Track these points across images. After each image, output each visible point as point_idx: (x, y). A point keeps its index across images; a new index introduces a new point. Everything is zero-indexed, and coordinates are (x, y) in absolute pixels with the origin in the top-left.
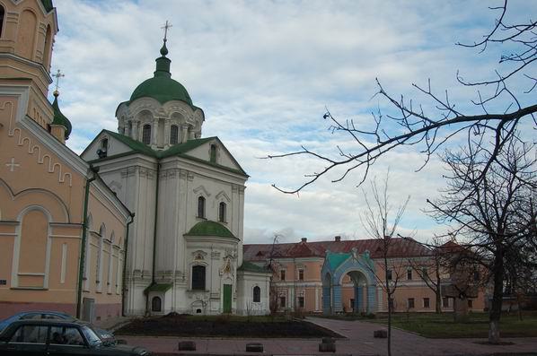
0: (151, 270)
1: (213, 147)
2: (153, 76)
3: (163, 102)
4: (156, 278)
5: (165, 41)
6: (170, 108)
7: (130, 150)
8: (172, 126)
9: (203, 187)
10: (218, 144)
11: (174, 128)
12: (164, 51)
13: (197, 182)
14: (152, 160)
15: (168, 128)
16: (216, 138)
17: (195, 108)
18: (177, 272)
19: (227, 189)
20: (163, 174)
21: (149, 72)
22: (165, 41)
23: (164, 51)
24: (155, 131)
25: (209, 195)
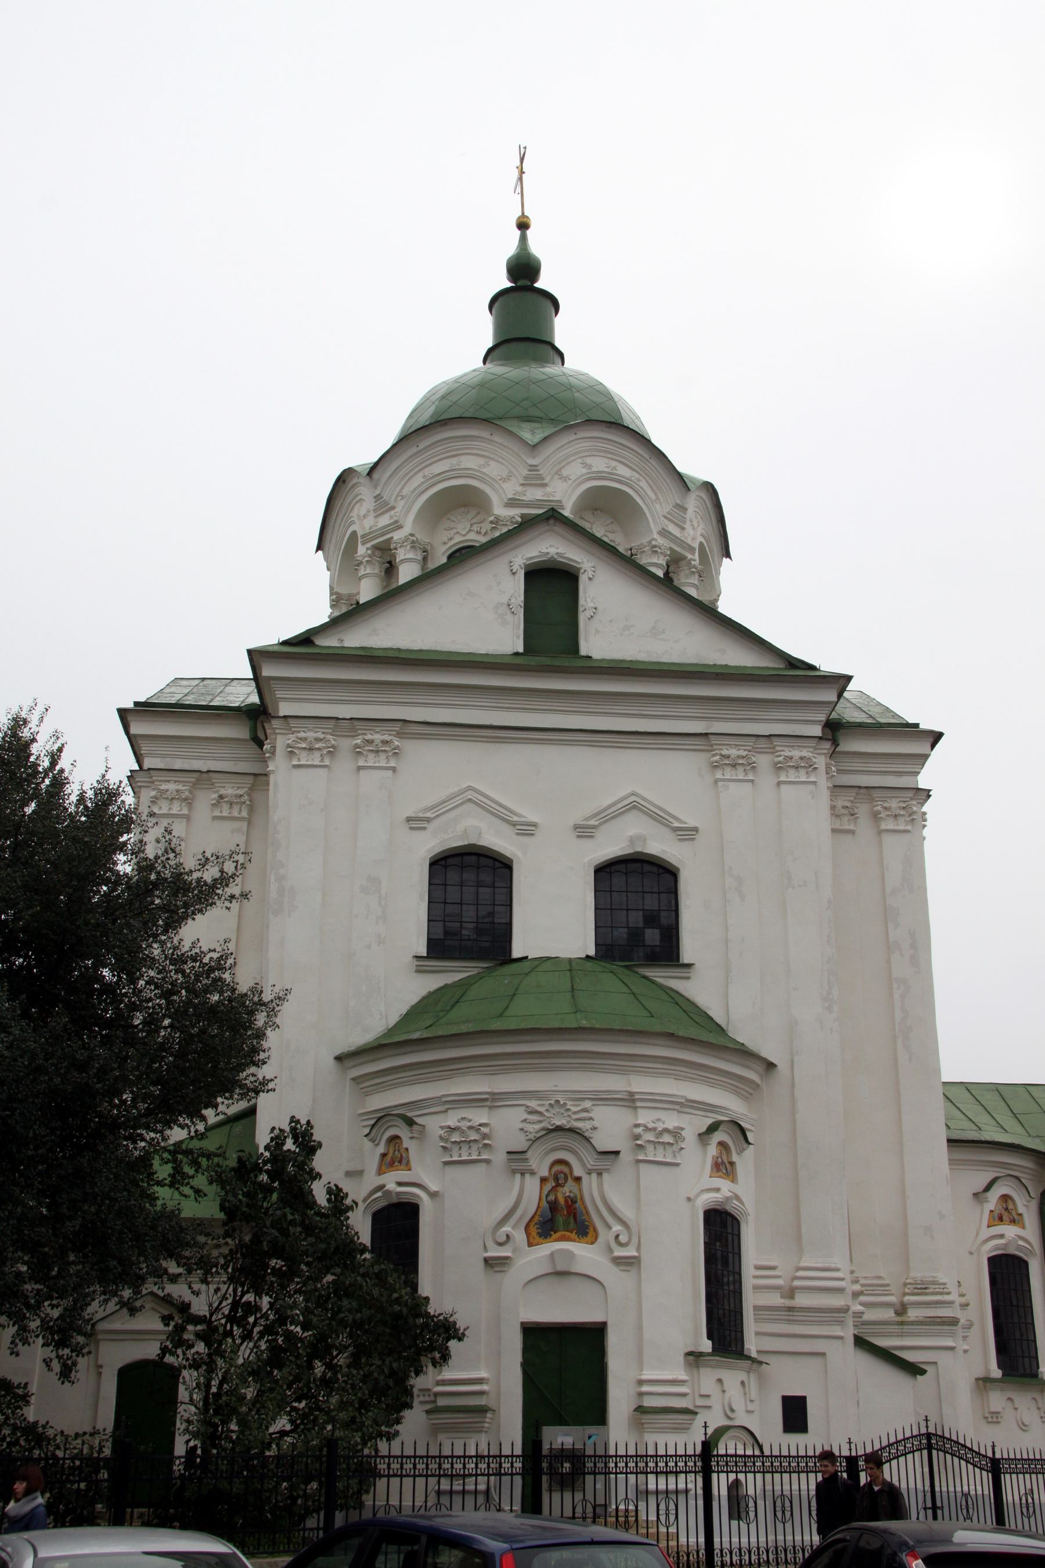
5: (523, 225)
12: (523, 269)
22: (523, 225)
23: (523, 269)
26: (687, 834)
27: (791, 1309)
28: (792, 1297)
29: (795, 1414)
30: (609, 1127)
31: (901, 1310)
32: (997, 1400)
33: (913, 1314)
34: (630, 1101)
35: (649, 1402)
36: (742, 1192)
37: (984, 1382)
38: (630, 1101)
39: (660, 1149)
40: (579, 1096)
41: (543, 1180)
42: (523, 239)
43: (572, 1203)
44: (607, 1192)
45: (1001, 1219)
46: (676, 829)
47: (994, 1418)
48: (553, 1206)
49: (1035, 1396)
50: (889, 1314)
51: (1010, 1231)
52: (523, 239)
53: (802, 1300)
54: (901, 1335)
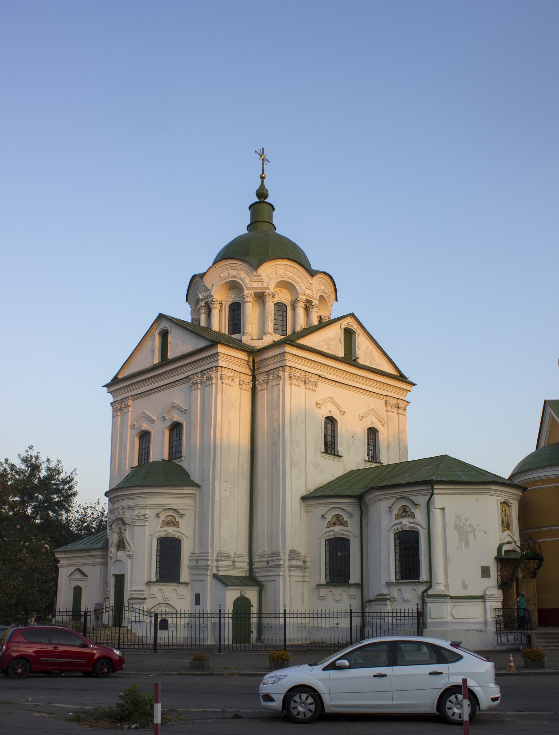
0: (243, 550)
1: (349, 333)
2: (247, 232)
3: (255, 266)
4: (256, 565)
5: (262, 178)
6: (273, 272)
7: (202, 344)
8: (277, 304)
9: (331, 400)
10: (355, 327)
11: (280, 307)
12: (262, 194)
13: (325, 390)
14: (243, 356)
15: (270, 306)
16: (352, 315)
17: (312, 273)
18: (294, 555)
19: (380, 404)
20: (261, 378)
21: (238, 225)
22: (262, 178)
23: (262, 194)
24: (251, 312)
25: (343, 413)
26: (184, 412)
27: (196, 566)
28: (197, 562)
29: (197, 599)
30: (128, 516)
31: (268, 562)
32: (324, 592)
33: (271, 563)
34: (132, 508)
35: (133, 596)
36: (185, 530)
37: (319, 586)
38: (132, 508)
39: (140, 521)
40: (123, 508)
41: (118, 533)
42: (262, 183)
43: (123, 539)
44: (127, 536)
45: (335, 524)
46: (182, 411)
47: (322, 598)
48: (120, 540)
49: (345, 589)
50: (265, 564)
51: (337, 529)
52: (262, 183)
53: (200, 563)
54: (267, 571)
